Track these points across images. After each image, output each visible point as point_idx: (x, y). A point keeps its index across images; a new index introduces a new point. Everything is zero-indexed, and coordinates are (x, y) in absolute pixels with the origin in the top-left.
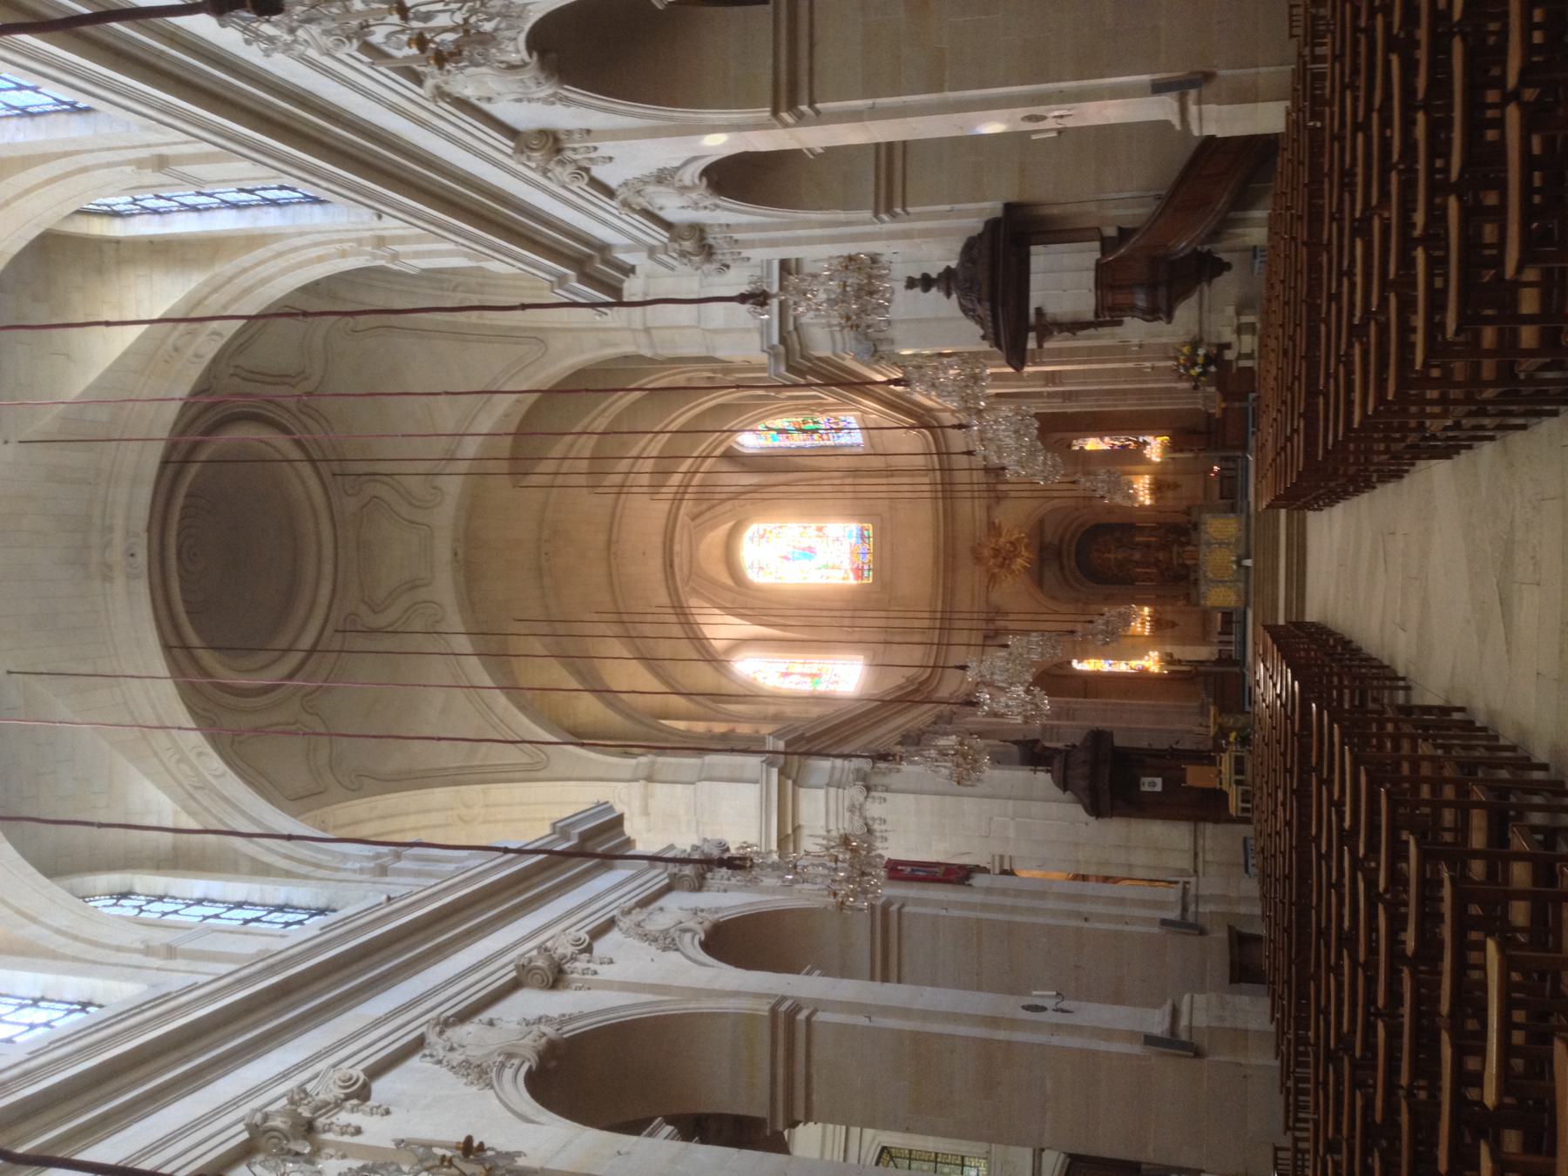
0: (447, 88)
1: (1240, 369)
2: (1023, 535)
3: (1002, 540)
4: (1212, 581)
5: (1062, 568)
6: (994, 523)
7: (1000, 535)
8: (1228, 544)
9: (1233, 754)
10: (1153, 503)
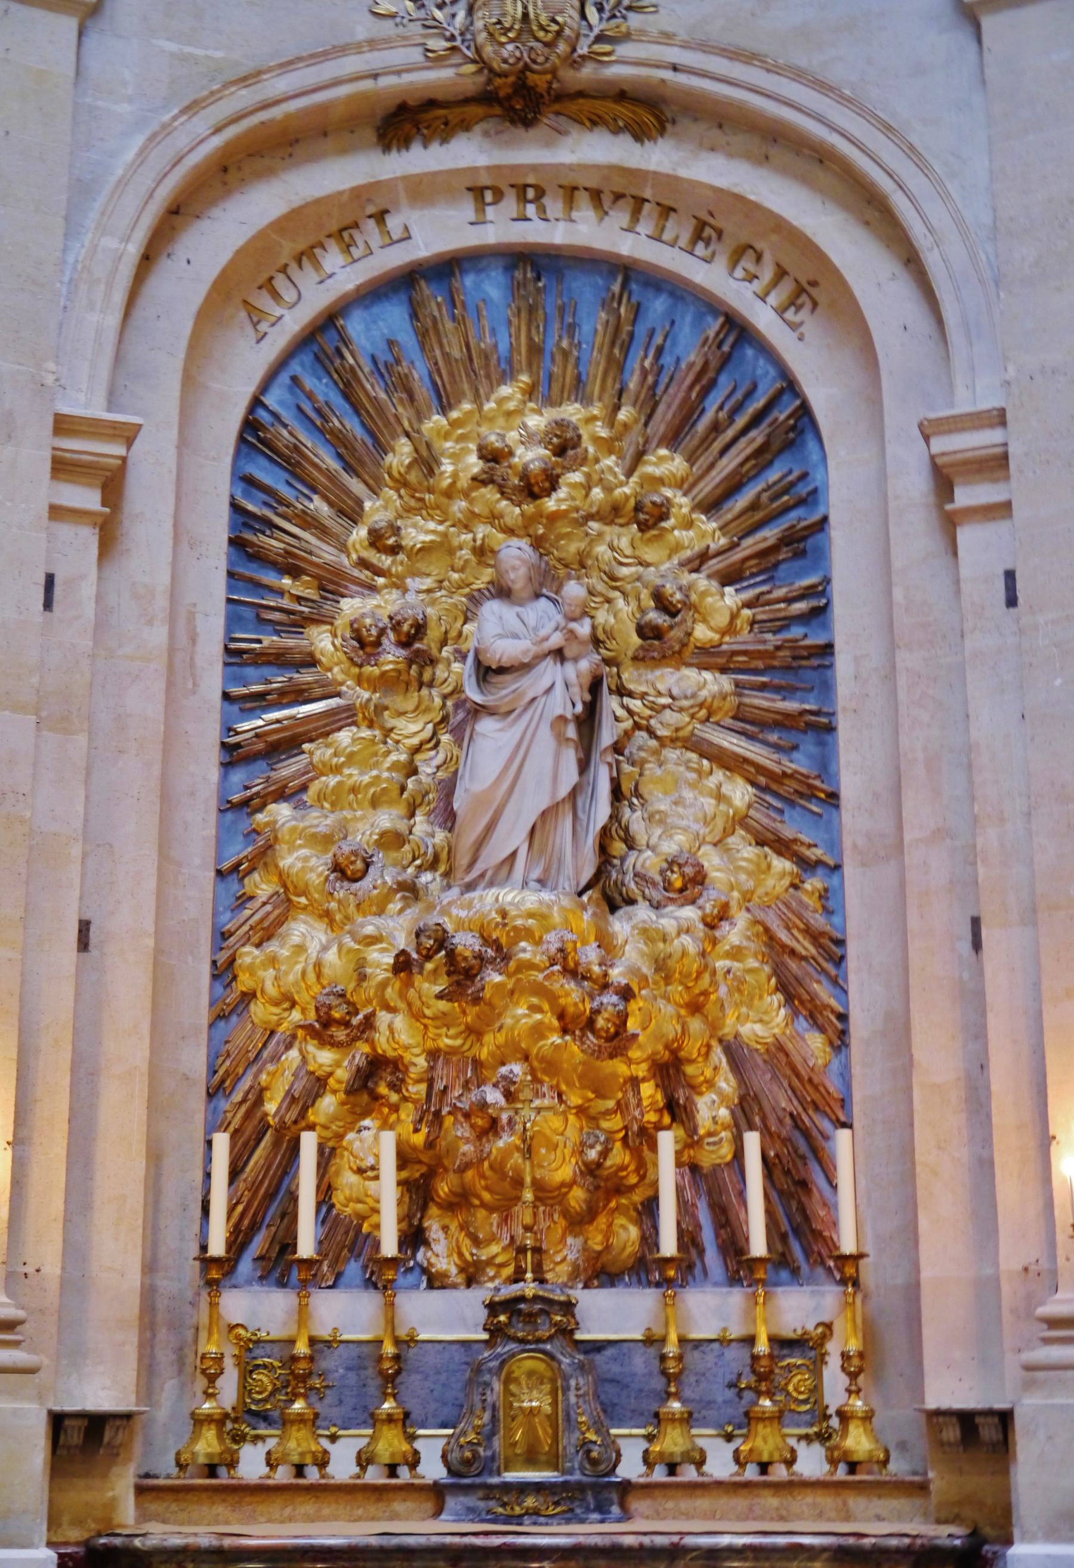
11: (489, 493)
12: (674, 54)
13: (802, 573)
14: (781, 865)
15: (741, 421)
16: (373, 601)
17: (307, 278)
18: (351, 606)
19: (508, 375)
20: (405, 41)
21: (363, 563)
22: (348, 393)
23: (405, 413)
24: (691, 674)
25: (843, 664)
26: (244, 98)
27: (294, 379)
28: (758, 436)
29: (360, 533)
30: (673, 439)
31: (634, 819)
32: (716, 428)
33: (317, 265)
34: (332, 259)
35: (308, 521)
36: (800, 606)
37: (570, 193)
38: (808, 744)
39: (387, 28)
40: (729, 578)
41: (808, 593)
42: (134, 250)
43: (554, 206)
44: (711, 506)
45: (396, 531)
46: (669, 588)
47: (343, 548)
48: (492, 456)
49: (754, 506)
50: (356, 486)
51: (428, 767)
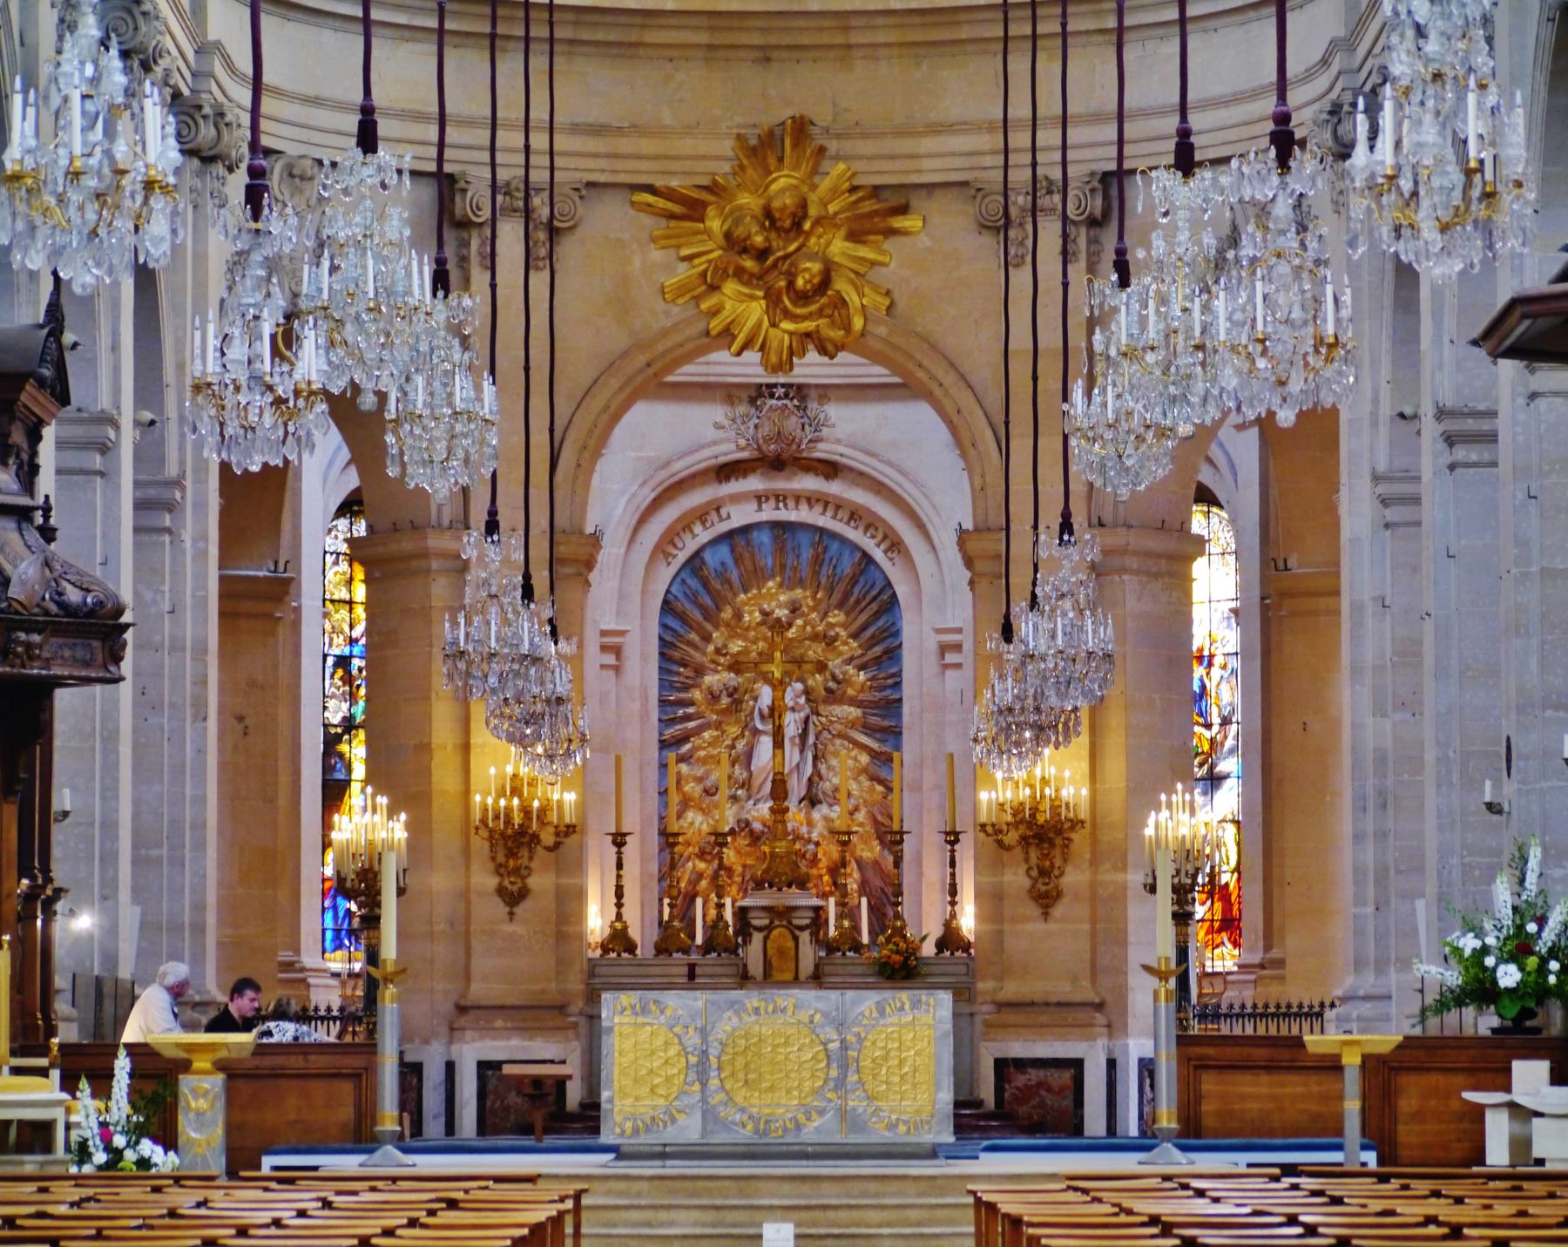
1: (1479, 1111)
2: (858, 323)
3: (838, 247)
4: (703, 1033)
5: (727, 471)
6: (903, 210)
7: (854, 237)
8: (840, 1084)
9: (58, 1114)
10: (983, 818)
11: (764, 629)
12: (841, 449)
13: (891, 666)
14: (880, 788)
15: (868, 599)
16: (717, 677)
17: (687, 537)
18: (709, 679)
19: (772, 577)
20: (728, 440)
21: (713, 662)
22: (705, 584)
23: (729, 595)
24: (846, 707)
25: (906, 708)
26: (664, 474)
27: (683, 581)
28: (874, 606)
29: (711, 648)
30: (840, 606)
31: (823, 768)
32: (858, 602)
33: (691, 531)
34: (698, 528)
35: (690, 644)
36: (890, 681)
37: (797, 499)
38: (892, 740)
39: (721, 434)
40: (861, 668)
41: (893, 675)
42: (623, 551)
43: (791, 504)
44: (855, 636)
45: (725, 646)
46: (837, 672)
47: (704, 654)
48: (765, 614)
49: (873, 637)
50: (709, 627)
51: (741, 745)
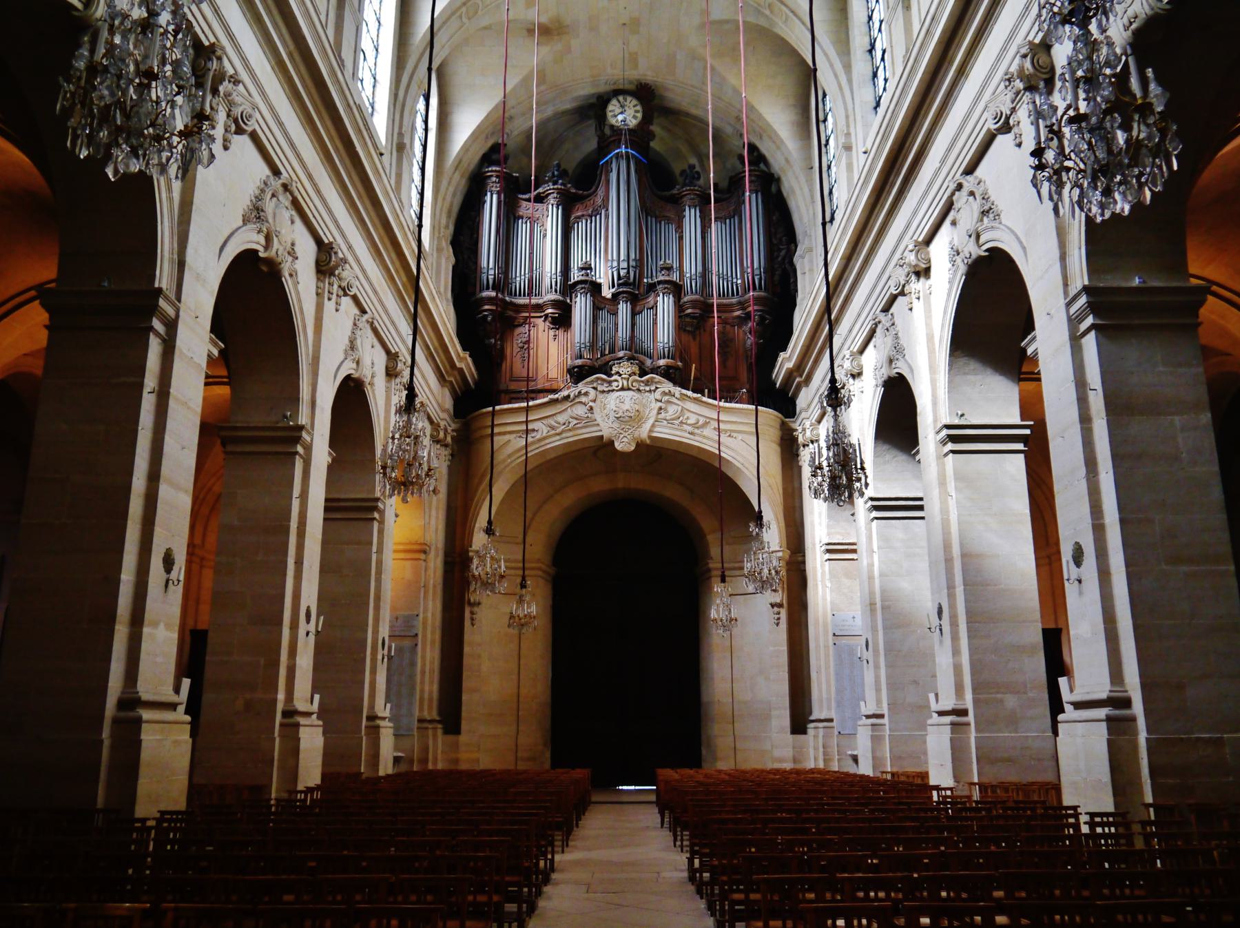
0: (880, 326)
